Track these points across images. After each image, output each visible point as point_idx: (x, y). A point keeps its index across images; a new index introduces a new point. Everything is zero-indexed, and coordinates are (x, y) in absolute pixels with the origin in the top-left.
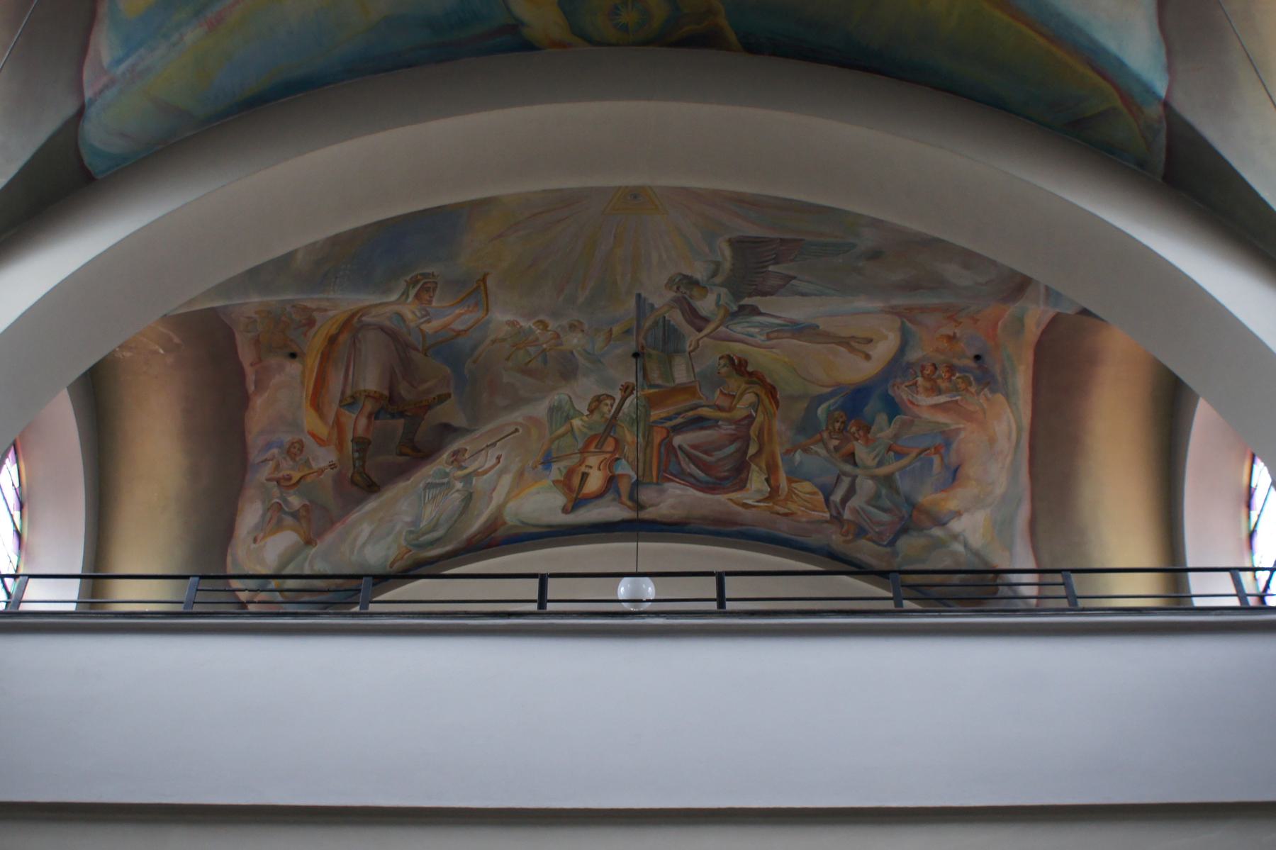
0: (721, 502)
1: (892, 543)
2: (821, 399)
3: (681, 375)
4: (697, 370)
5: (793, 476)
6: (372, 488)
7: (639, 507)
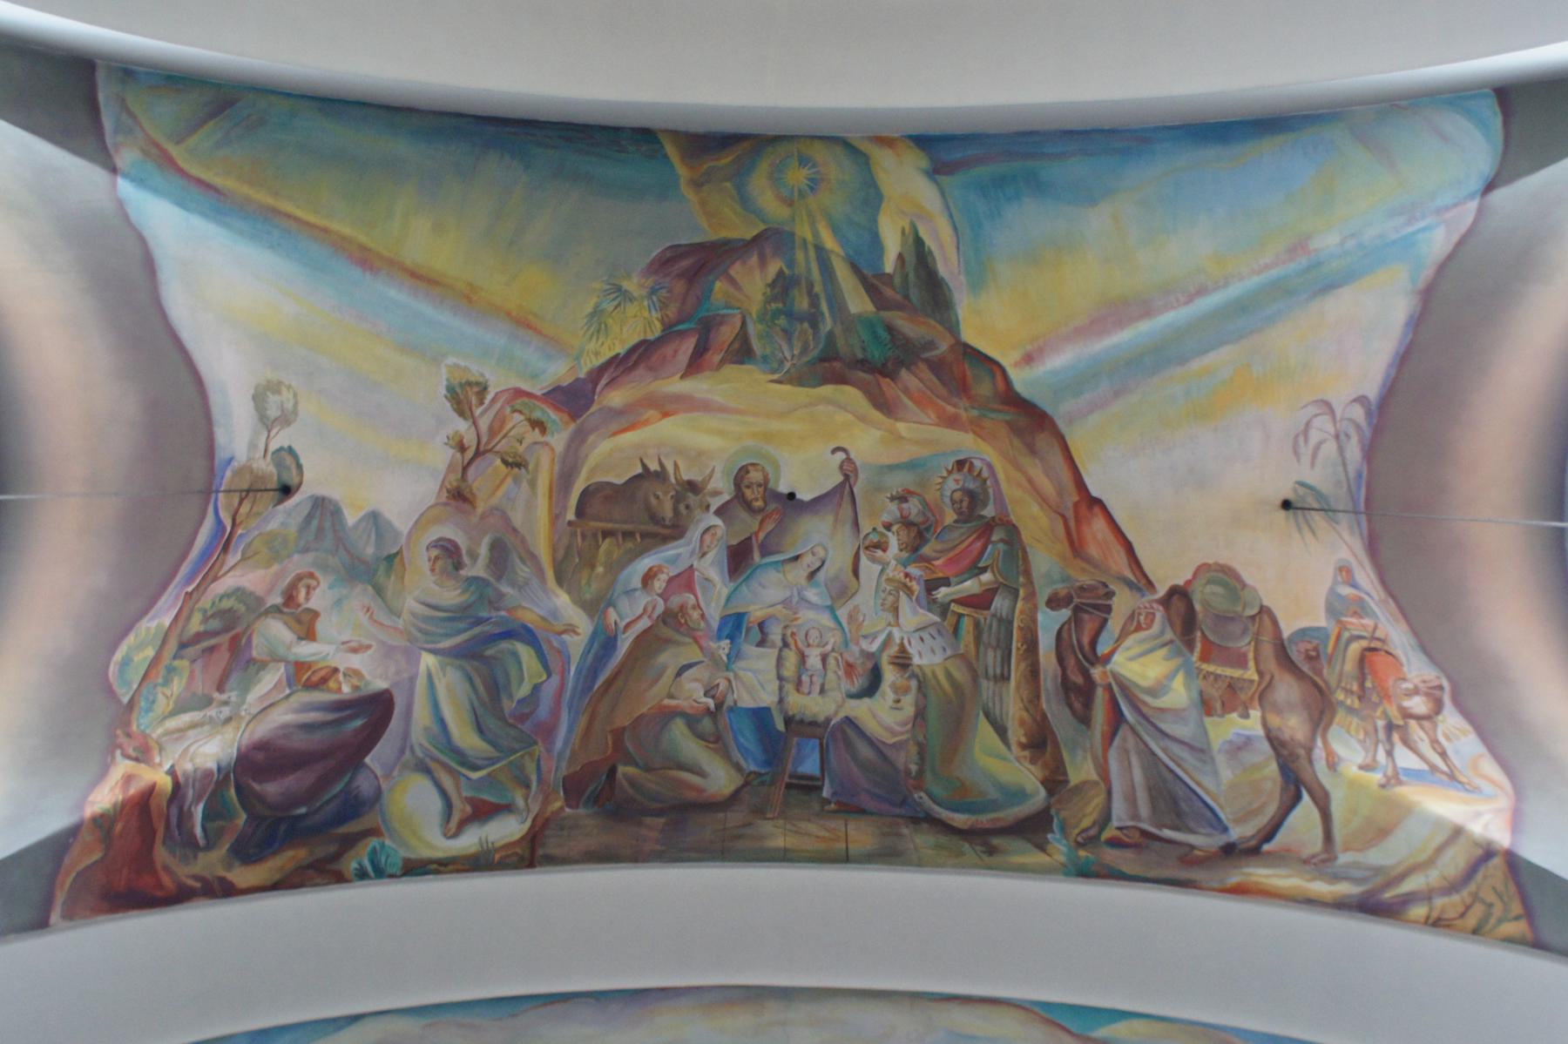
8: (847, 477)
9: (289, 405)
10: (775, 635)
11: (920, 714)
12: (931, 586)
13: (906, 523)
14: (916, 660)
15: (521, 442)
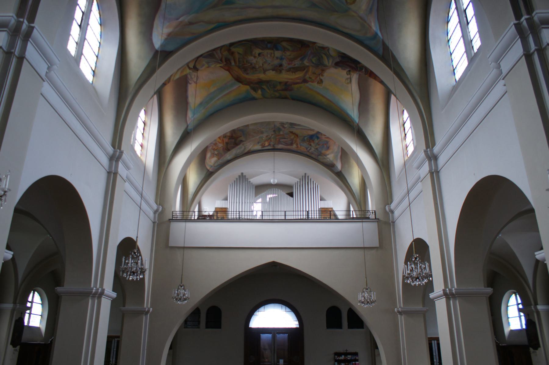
0: (289, 147)
1: (318, 156)
2: (305, 137)
3: (281, 133)
6: (229, 150)
7: (274, 147)
10: (275, 58)
14: (253, 58)
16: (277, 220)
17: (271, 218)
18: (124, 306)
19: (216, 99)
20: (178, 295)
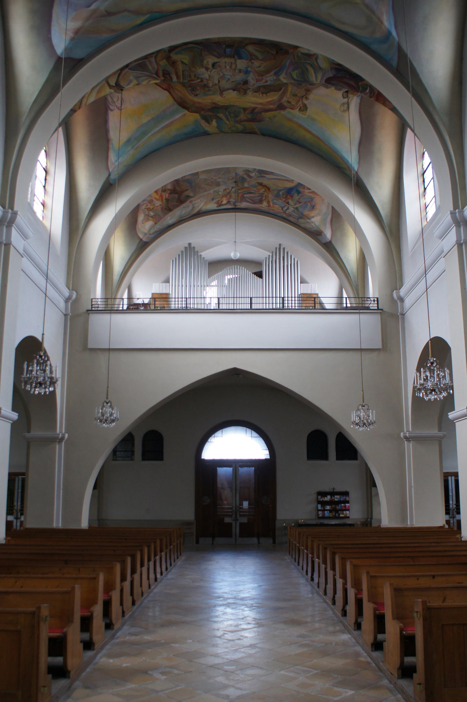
0: (257, 206)
1: (298, 219)
2: (280, 191)
3: (246, 185)
4: (250, 185)
5: (274, 204)
6: (170, 210)
7: (236, 206)
8: (222, 93)
9: (342, 107)
10: (237, 71)
11: (202, 61)
12: (202, 81)
13: (208, 87)
14: (204, 70)
15: (293, 99)
16: (239, 309)
17: (231, 307)
18: (29, 431)
19: (149, 135)
20: (103, 415)
